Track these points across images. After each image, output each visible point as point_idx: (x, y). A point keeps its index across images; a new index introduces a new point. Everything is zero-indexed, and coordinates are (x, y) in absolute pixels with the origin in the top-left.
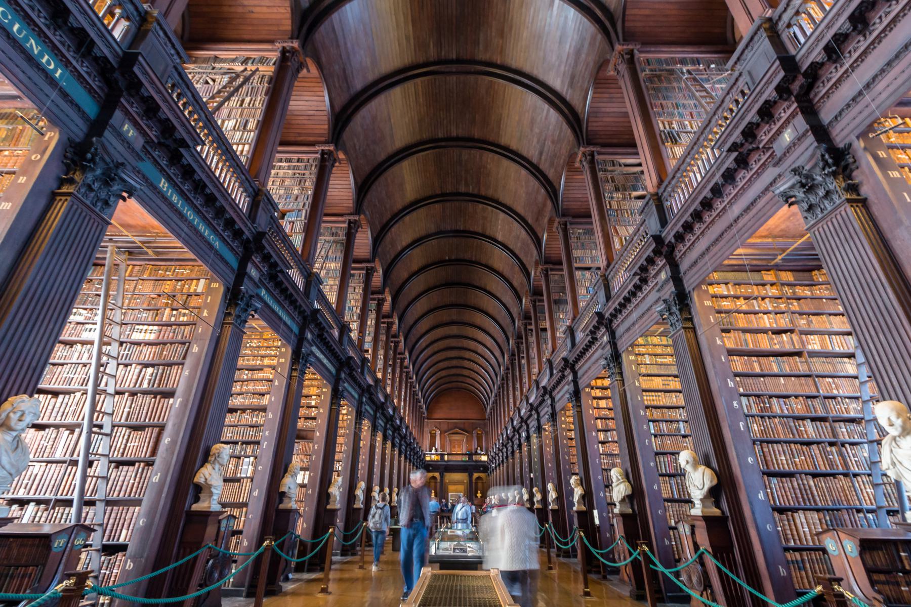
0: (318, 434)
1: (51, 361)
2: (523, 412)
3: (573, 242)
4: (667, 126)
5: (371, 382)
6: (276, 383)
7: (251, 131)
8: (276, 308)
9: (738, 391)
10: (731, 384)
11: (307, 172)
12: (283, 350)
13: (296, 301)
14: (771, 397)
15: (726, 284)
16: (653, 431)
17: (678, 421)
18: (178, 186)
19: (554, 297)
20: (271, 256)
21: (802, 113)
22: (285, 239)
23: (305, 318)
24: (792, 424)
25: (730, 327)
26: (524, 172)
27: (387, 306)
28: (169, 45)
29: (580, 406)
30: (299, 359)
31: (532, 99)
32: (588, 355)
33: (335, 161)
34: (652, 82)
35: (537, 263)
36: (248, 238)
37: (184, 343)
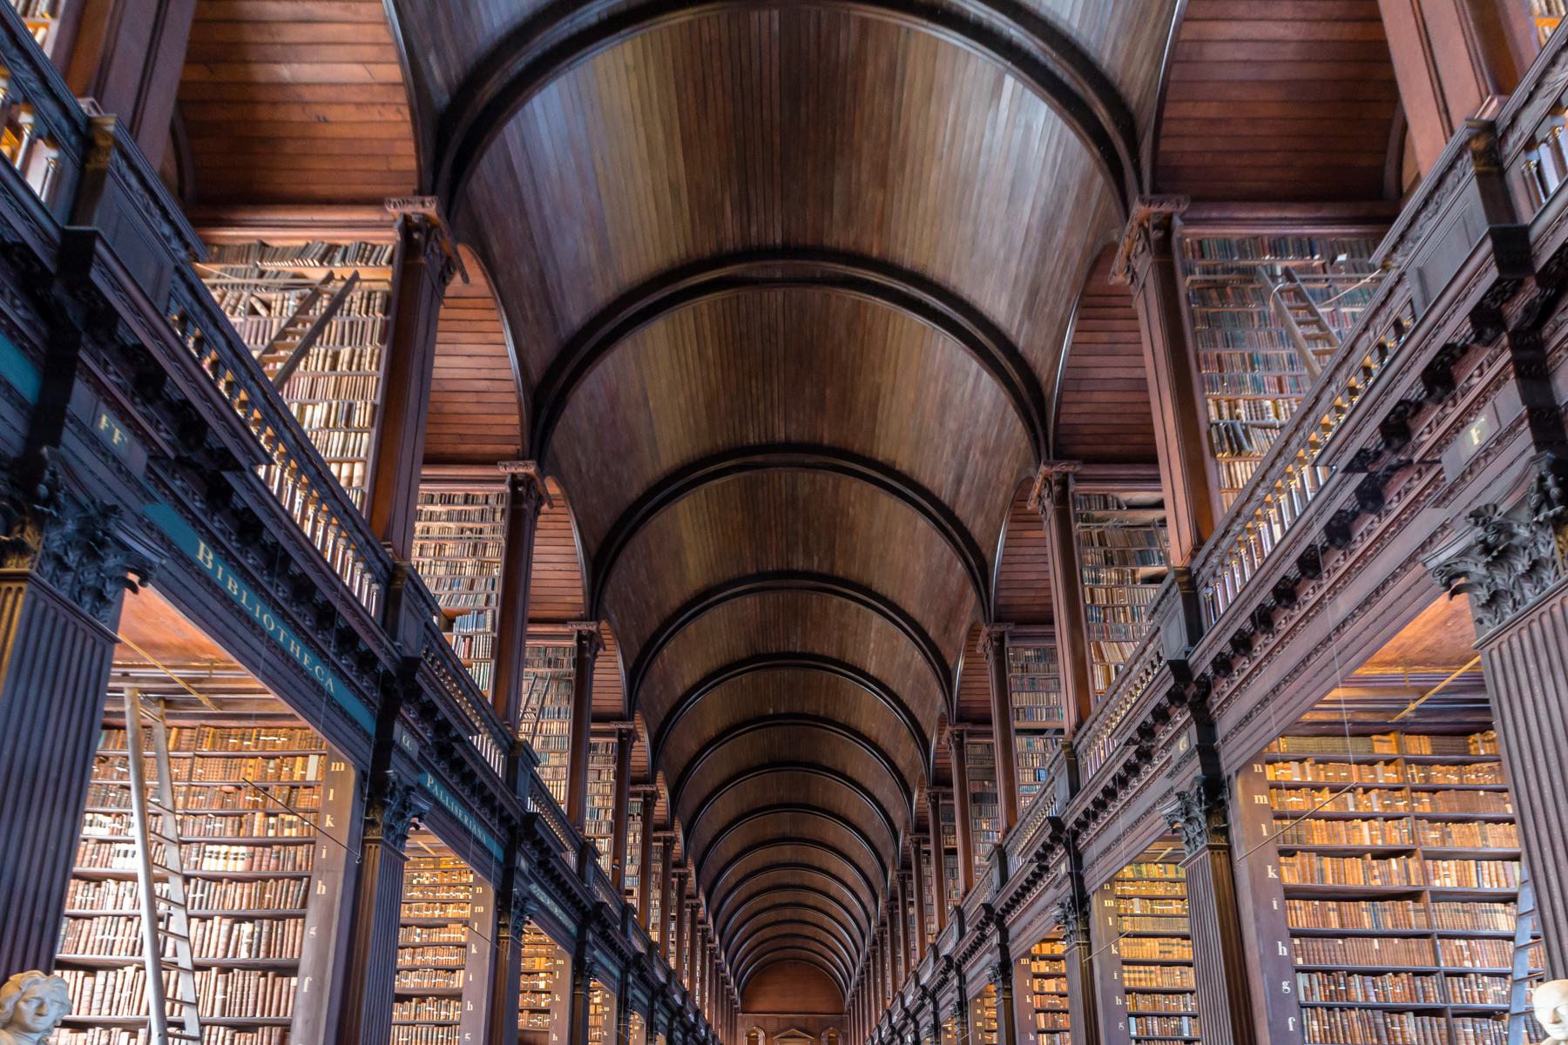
0: (555, 1038)
1: (67, 911)
2: (909, 1000)
3: (1014, 675)
4: (1225, 412)
5: (641, 948)
6: (474, 951)
7: (361, 430)
8: (458, 811)
9: (1293, 962)
10: (1283, 950)
11: (487, 527)
12: (479, 890)
13: (493, 797)
14: (1350, 973)
15: (1301, 761)
16: (1134, 1033)
17: (1180, 1016)
18: (235, 559)
19: (974, 788)
20: (436, 709)
21: (1519, 375)
22: (459, 672)
23: (512, 831)
24: (1380, 1020)
25: (1296, 845)
26: (922, 523)
27: (661, 808)
28: (156, 211)
29: (1010, 990)
30: (509, 907)
31: (946, 350)
32: (1029, 898)
33: (541, 499)
34: (1204, 301)
35: (942, 721)
36: (387, 671)
37: (299, 879)
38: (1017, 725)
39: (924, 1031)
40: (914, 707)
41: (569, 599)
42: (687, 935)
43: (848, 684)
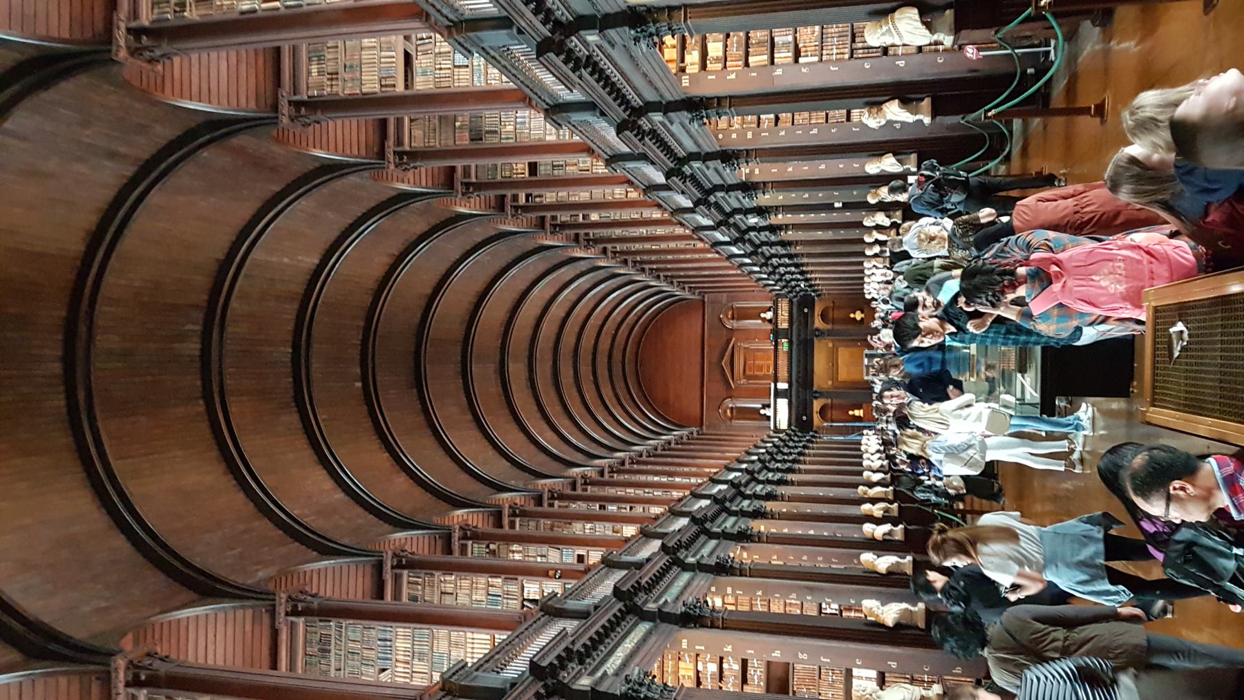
26: (154, 198)
38: (400, 88)
39: (748, 203)
40: (359, 210)
41: (248, 627)
42: (620, 492)
43: (329, 291)
